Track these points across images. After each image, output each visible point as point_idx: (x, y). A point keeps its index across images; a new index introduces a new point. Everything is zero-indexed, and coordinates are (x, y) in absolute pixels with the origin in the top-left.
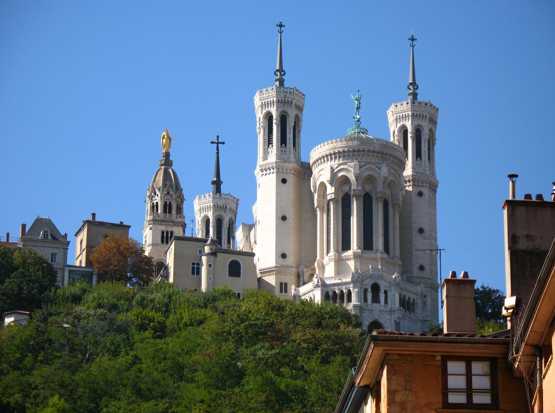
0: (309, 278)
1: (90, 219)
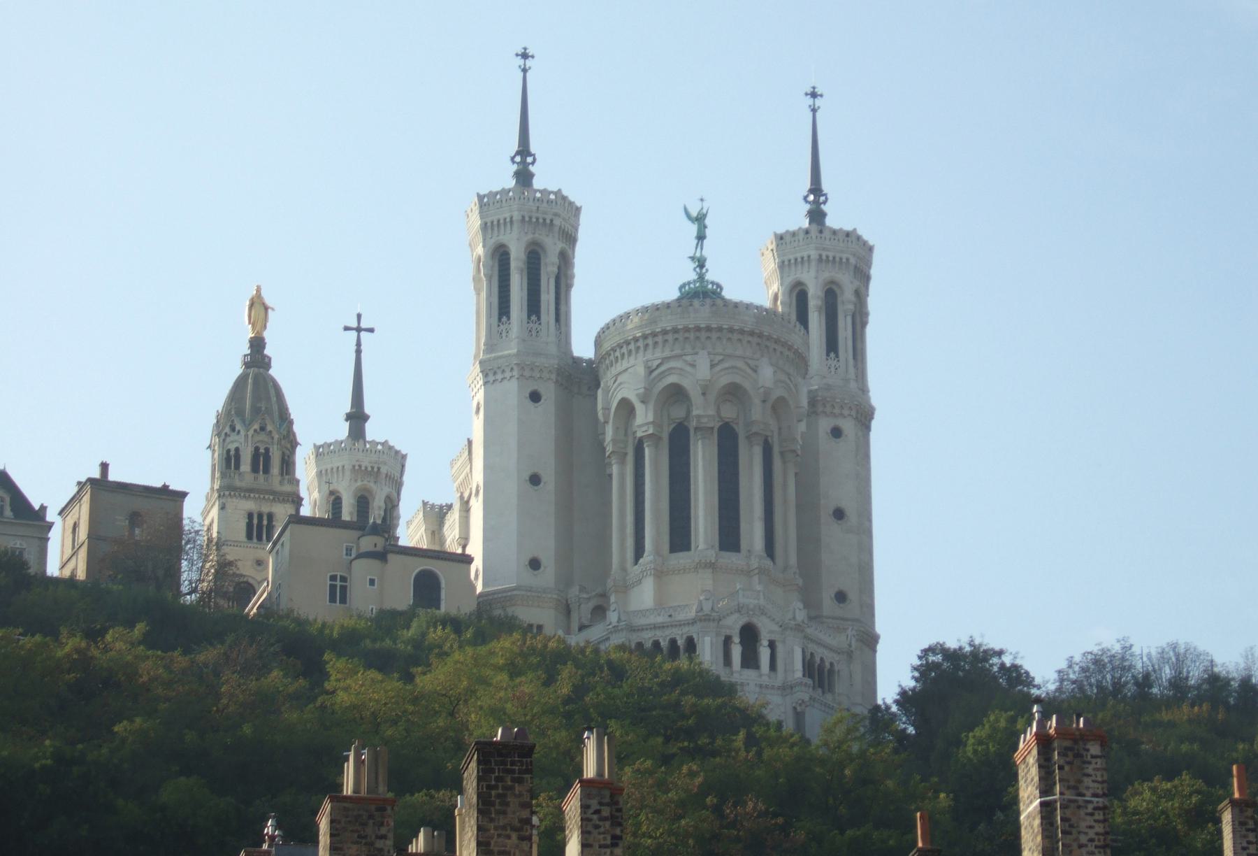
0: (591, 614)
1: (96, 474)
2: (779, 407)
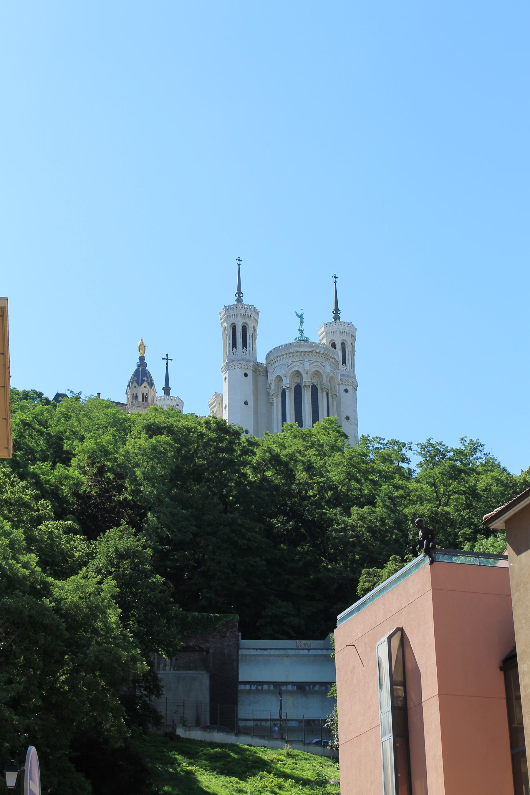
2: (331, 379)
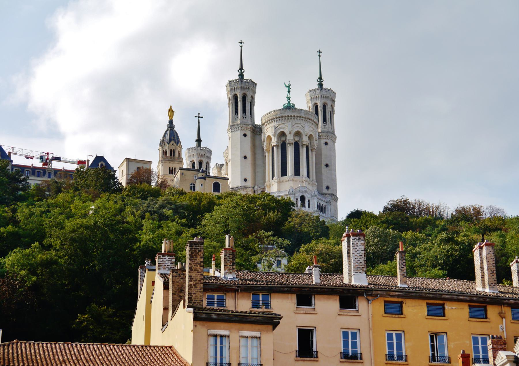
2: (310, 137)
